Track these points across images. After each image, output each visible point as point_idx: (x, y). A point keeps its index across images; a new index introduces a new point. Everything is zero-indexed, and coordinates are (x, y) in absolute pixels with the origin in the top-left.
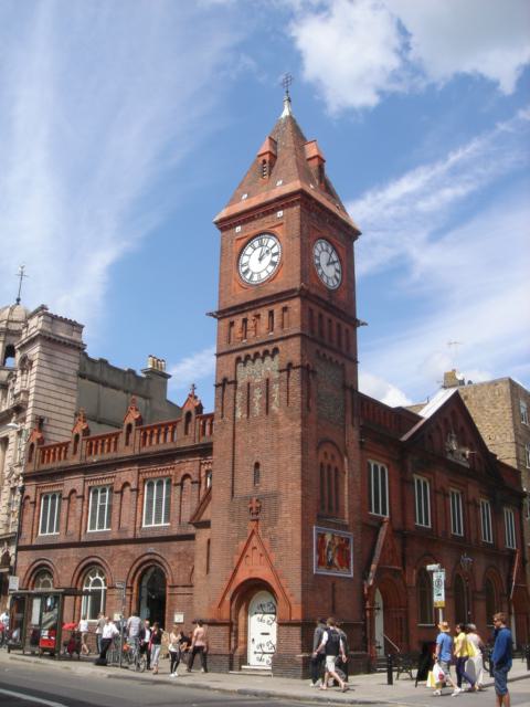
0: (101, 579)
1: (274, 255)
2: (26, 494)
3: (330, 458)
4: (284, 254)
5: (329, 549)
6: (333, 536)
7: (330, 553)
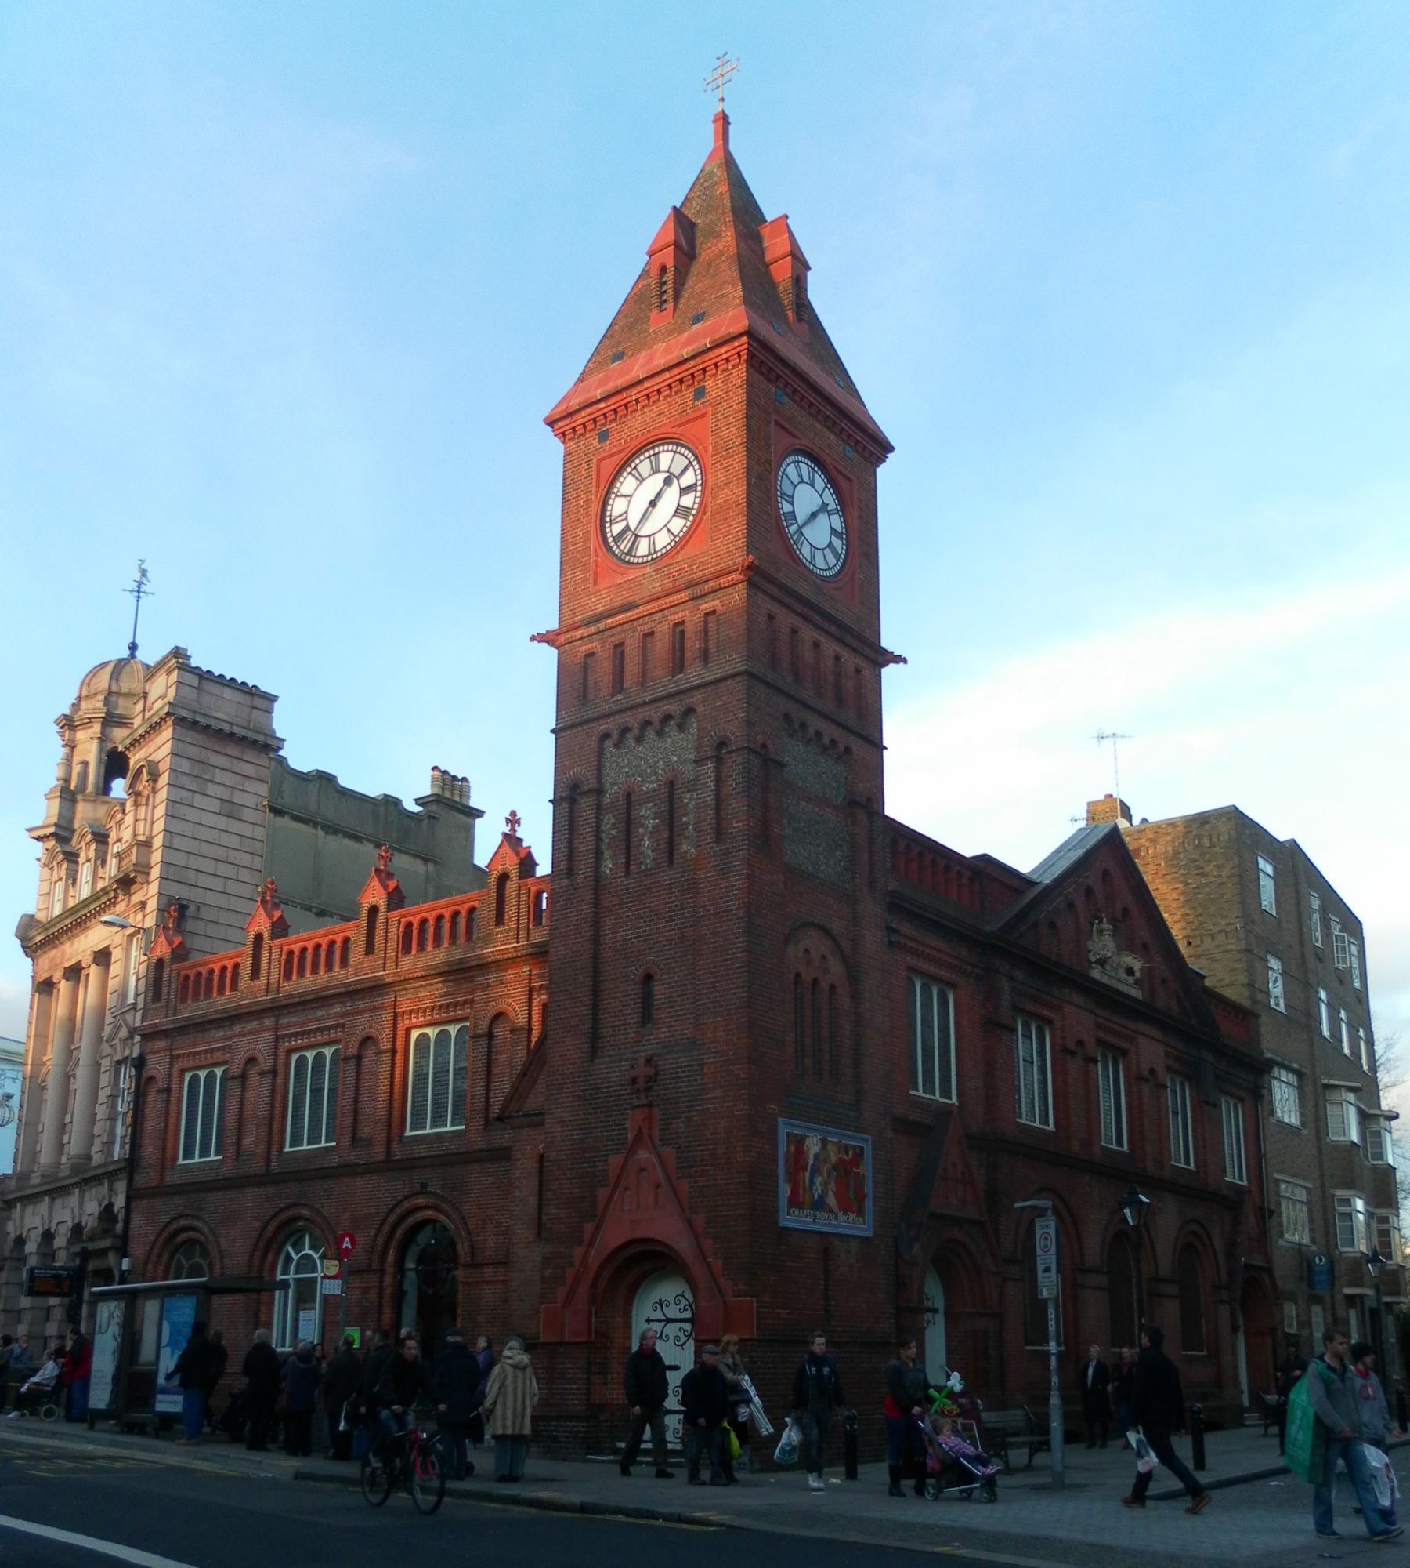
1: (684, 491)
2: (146, 1074)
4: (704, 485)
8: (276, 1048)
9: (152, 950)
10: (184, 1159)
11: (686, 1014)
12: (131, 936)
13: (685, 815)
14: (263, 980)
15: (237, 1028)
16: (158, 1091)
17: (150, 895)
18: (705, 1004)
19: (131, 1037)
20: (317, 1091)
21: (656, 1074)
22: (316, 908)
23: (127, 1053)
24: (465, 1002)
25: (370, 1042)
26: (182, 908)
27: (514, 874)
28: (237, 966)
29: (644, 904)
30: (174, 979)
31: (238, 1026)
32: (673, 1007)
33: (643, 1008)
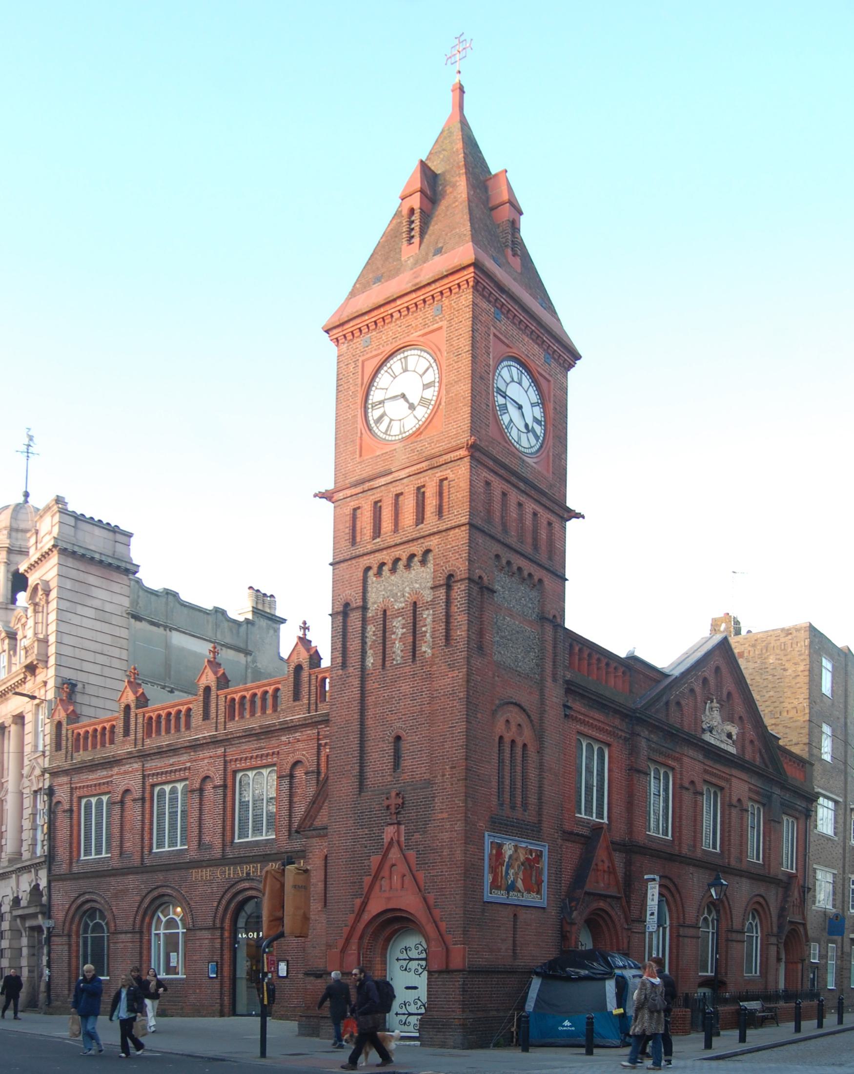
0: (178, 919)
2: (54, 801)
3: (514, 728)
5: (509, 866)
6: (516, 847)
7: (511, 871)
8: (144, 783)
9: (53, 715)
10: (85, 856)
11: (423, 763)
12: (38, 705)
13: (425, 626)
14: (132, 737)
15: (116, 770)
16: (64, 811)
17: (49, 676)
18: (437, 756)
19: (43, 775)
20: (173, 814)
21: (403, 803)
22: (169, 687)
23: (41, 785)
24: (273, 753)
25: (208, 780)
26: (72, 686)
27: (306, 666)
28: (113, 727)
29: (396, 688)
30: (70, 736)
31: (116, 768)
32: (415, 758)
33: (395, 759)
